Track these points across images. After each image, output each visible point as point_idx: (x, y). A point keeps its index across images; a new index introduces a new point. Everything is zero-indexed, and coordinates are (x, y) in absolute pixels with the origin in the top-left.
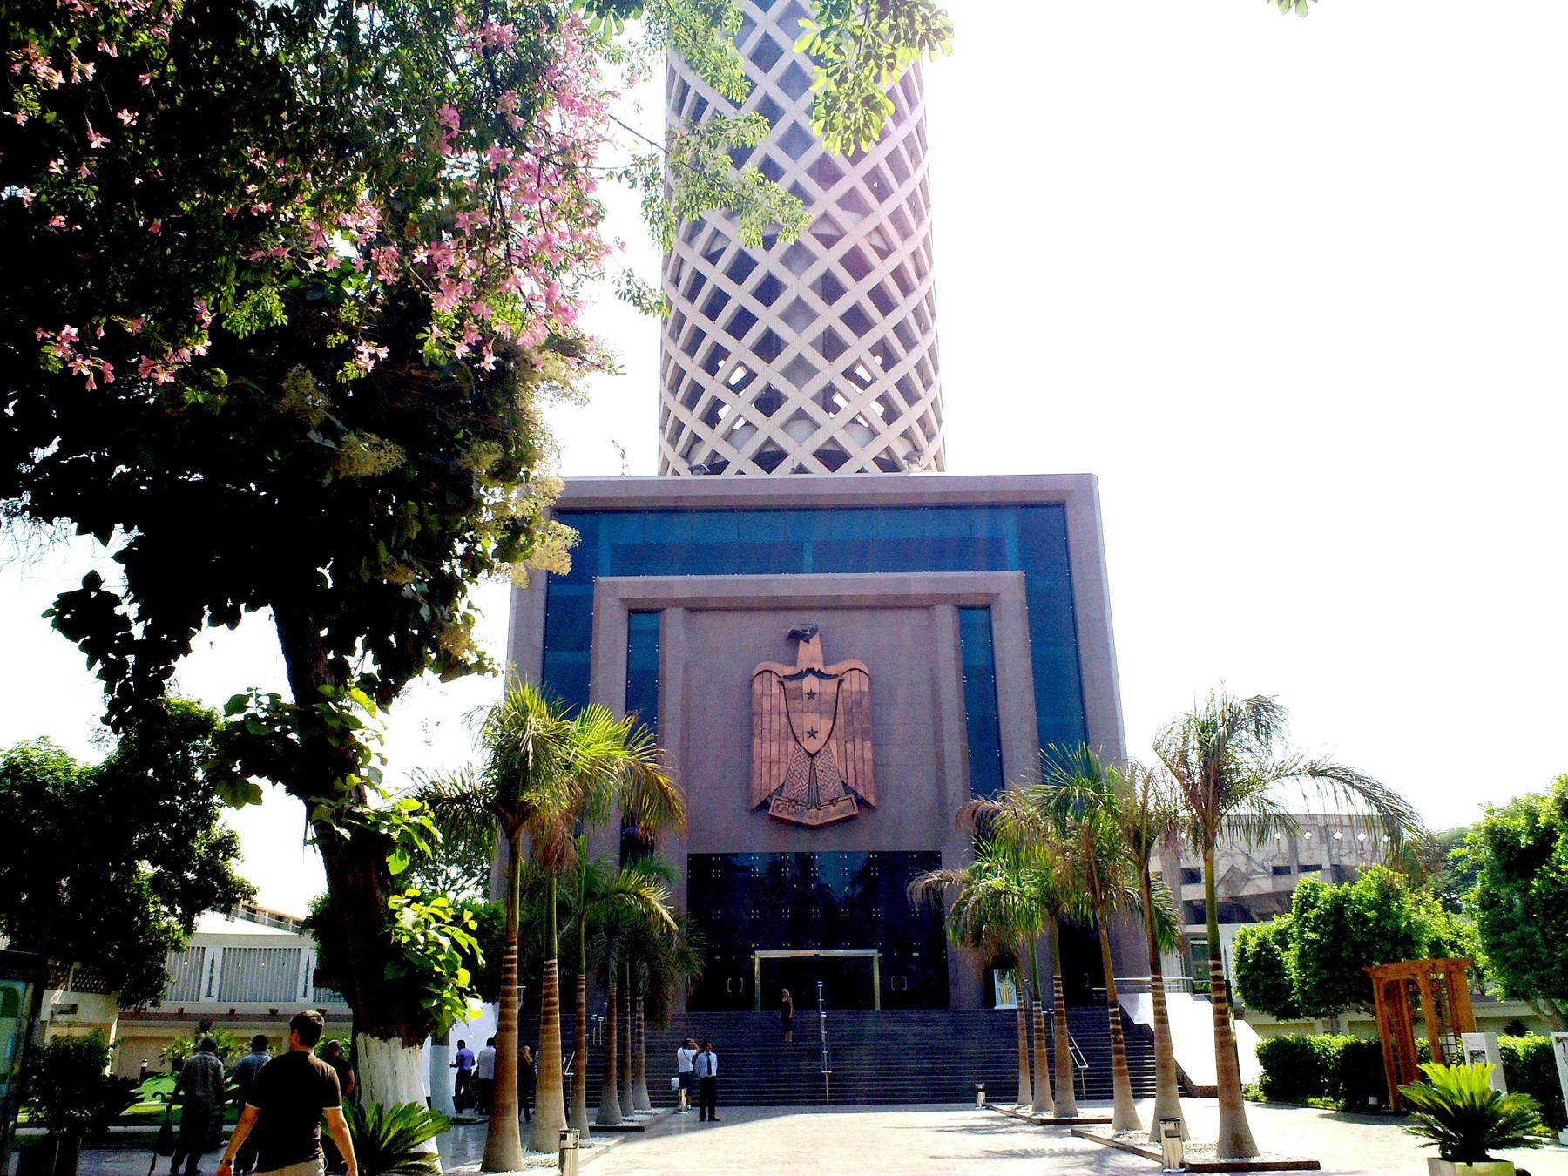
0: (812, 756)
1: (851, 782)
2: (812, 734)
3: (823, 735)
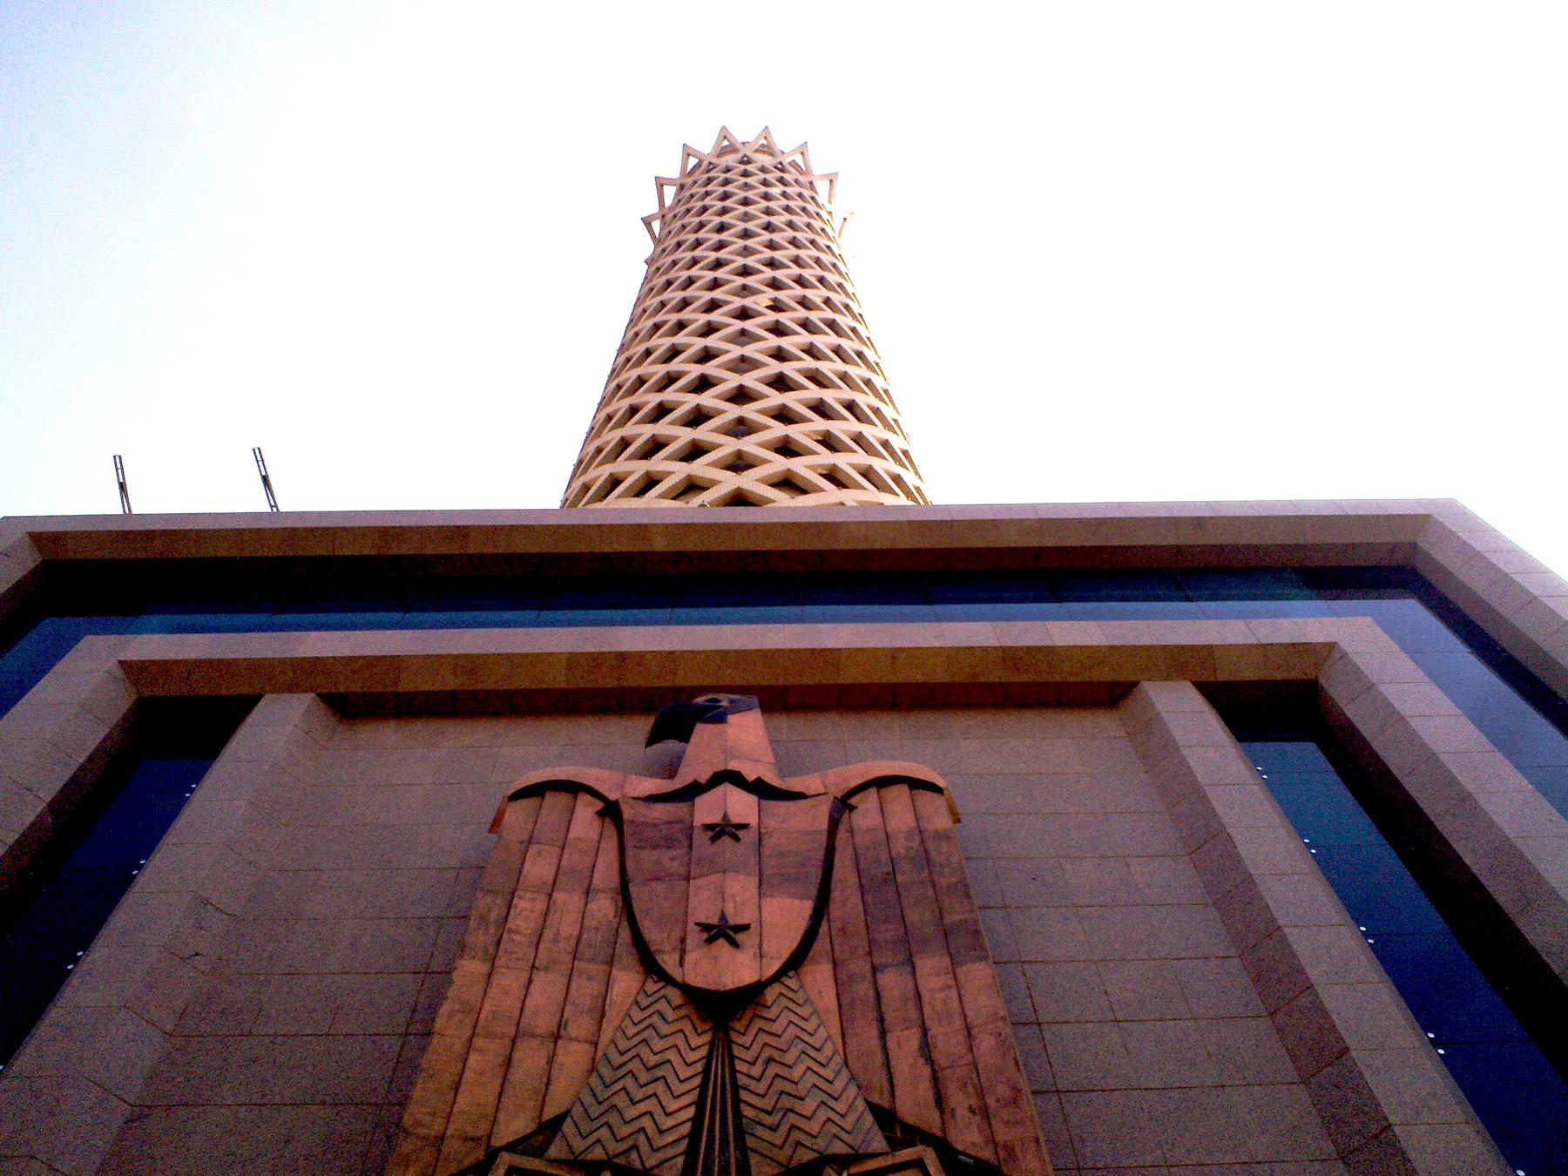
0: (722, 1011)
1: (914, 1104)
2: (723, 932)
3: (782, 946)
